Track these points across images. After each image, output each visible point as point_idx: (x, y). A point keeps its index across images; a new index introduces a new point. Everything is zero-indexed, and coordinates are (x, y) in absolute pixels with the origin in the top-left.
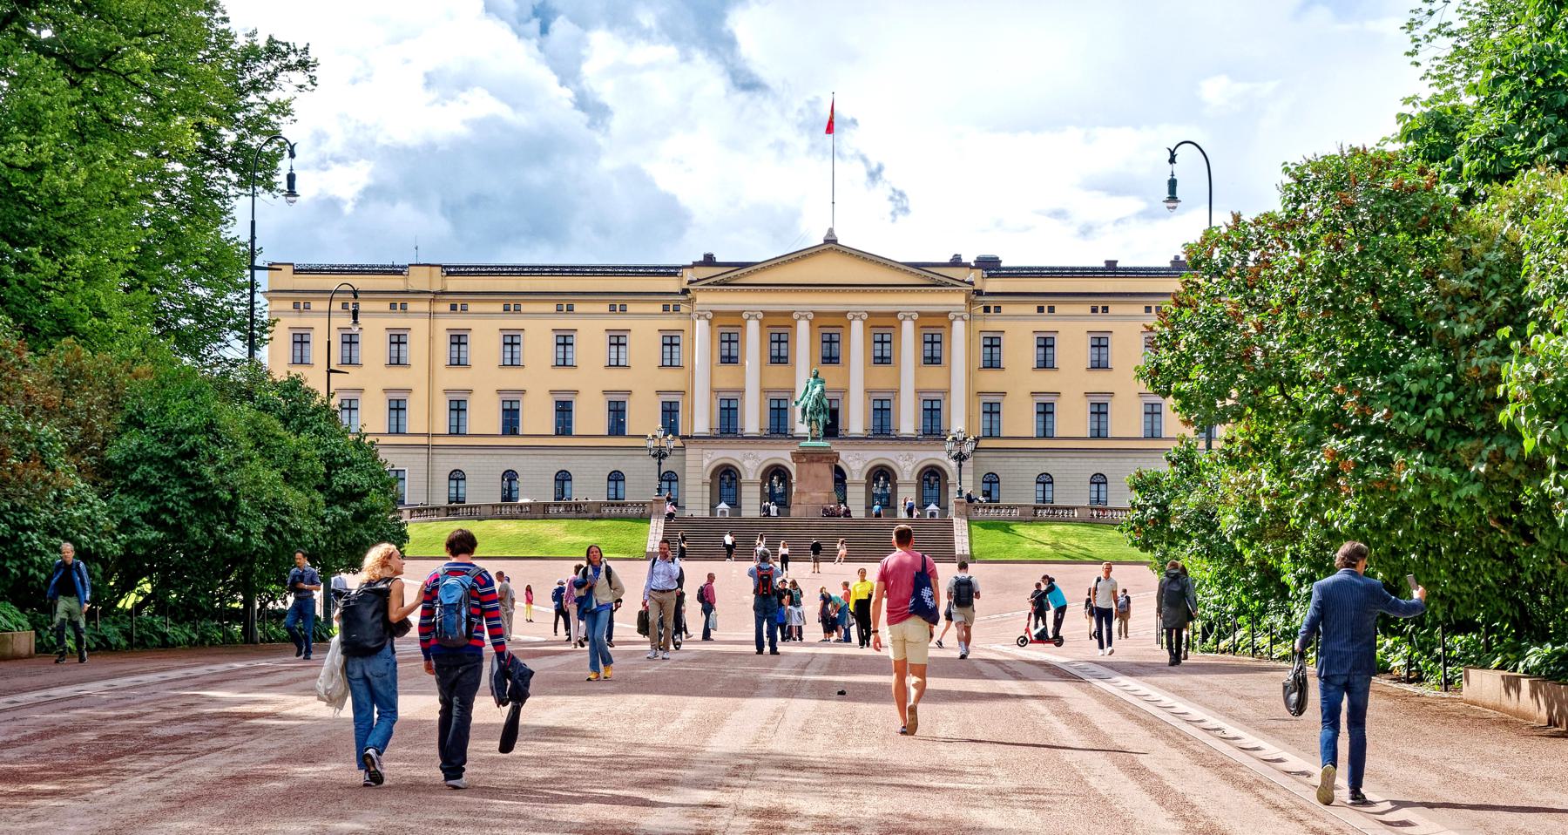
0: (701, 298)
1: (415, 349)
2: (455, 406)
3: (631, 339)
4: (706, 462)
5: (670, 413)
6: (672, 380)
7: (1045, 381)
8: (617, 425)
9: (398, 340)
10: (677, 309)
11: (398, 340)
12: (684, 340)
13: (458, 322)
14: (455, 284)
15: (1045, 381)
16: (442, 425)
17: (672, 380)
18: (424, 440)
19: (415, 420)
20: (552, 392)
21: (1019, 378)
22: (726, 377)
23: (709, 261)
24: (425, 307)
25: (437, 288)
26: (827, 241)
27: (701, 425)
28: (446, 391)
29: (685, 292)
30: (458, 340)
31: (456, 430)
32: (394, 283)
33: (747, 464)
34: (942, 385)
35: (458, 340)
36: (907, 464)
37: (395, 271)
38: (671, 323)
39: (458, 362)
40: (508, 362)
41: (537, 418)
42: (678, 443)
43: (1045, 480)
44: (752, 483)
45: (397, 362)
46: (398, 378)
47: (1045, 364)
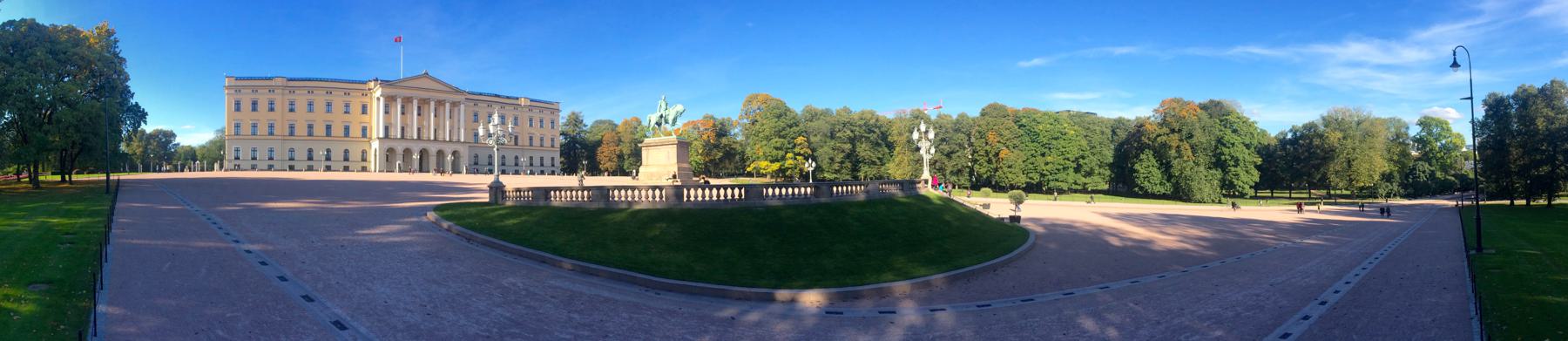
1: (277, 107)
13: (292, 97)
16: (287, 132)
39: (292, 110)
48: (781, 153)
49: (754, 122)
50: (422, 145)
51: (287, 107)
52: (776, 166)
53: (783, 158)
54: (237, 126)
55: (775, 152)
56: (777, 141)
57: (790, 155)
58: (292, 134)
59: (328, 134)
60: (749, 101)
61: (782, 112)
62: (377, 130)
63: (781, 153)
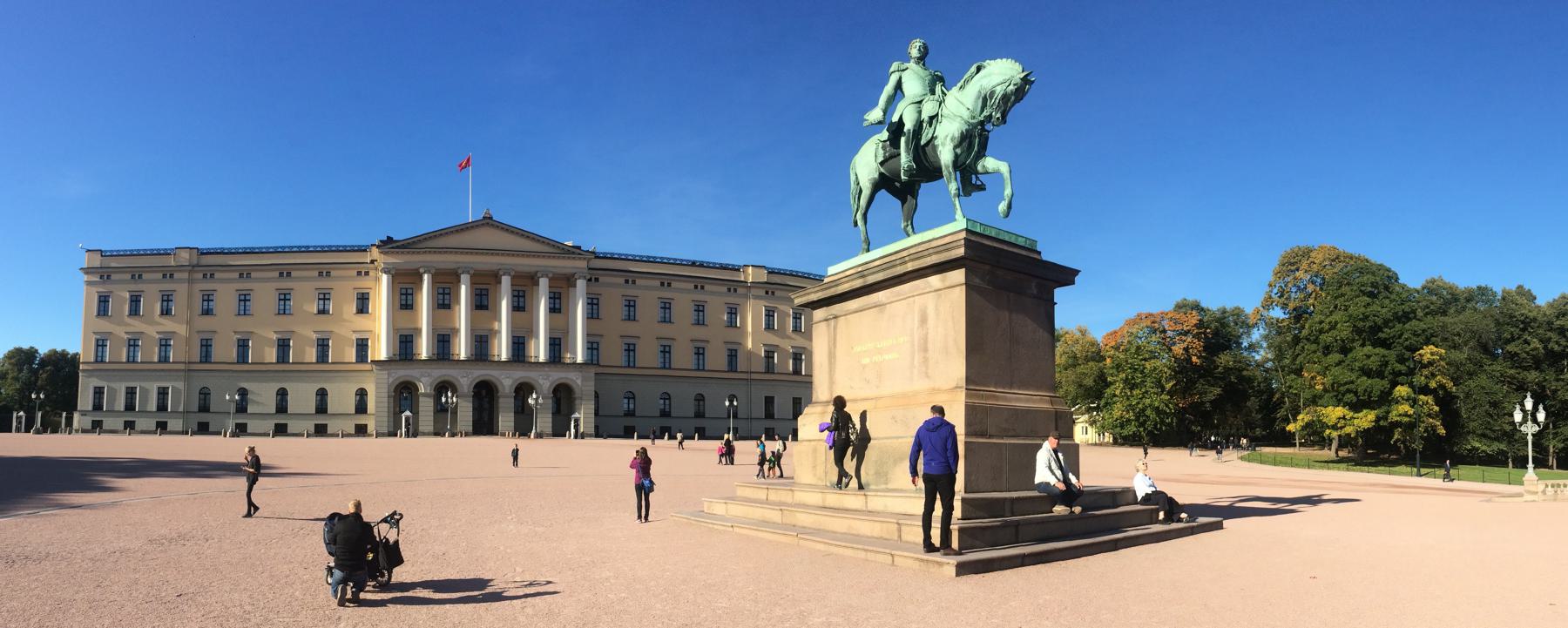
10: (367, 273)
16: (196, 355)
18: (182, 367)
23: (390, 239)
38: (364, 283)
39: (207, 312)
43: (631, 396)
44: (425, 395)
45: (166, 312)
48: (1379, 385)
49: (1299, 315)
50: (558, 376)
51: (198, 305)
52: (1366, 419)
53: (1386, 399)
54: (101, 344)
55: (1364, 382)
56: (1366, 353)
57: (1402, 390)
58: (206, 357)
59: (242, 357)
60: (1290, 264)
61: (1380, 283)
62: (381, 349)
63: (1379, 385)
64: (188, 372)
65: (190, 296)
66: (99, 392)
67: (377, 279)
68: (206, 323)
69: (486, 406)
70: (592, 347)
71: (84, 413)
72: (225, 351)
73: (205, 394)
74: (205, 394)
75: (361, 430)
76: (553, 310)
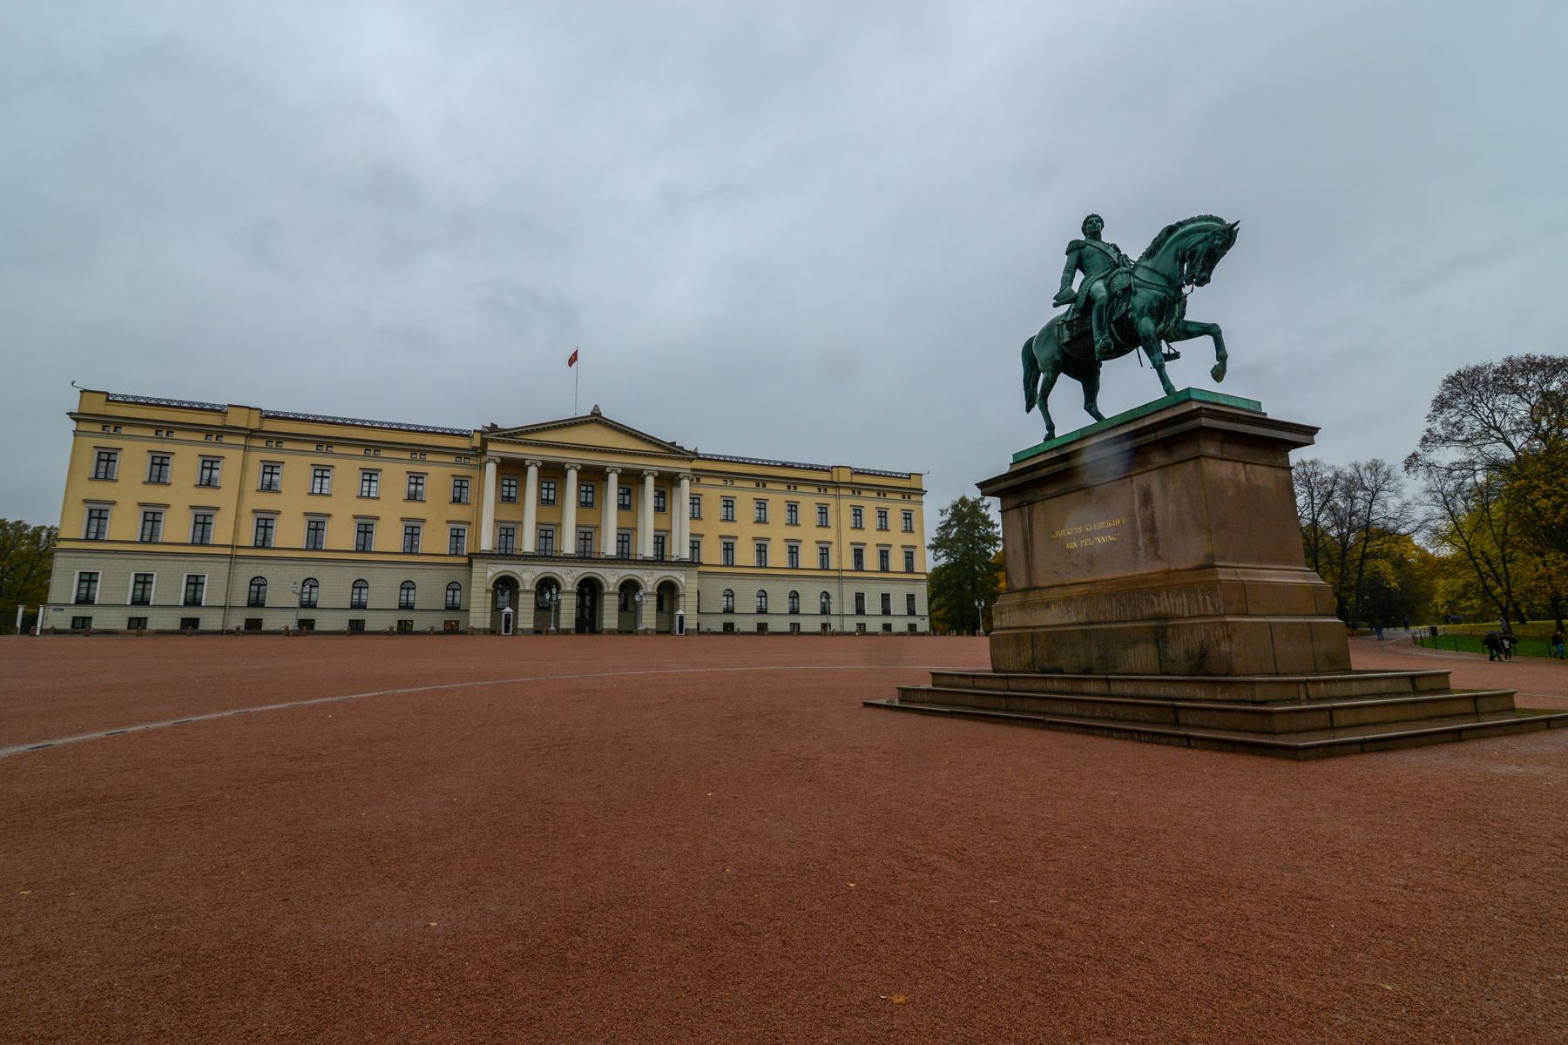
0: (491, 447)
1: (228, 473)
2: (262, 523)
3: (427, 480)
4: (490, 574)
5: (457, 536)
6: (458, 512)
7: (728, 529)
8: (411, 547)
9: (210, 463)
11: (210, 463)
12: (472, 484)
14: (270, 426)
15: (728, 529)
16: (248, 537)
17: (458, 512)
18: (228, 551)
19: (221, 532)
20: (355, 517)
21: (713, 530)
22: (508, 513)
24: (241, 441)
25: (254, 425)
26: (593, 414)
27: (486, 544)
28: (254, 511)
29: (474, 449)
30: (270, 468)
31: (263, 543)
32: (214, 420)
33: (525, 576)
34: (666, 527)
35: (270, 468)
36: (650, 580)
37: (213, 410)
39: (269, 488)
40: (317, 491)
41: (341, 536)
42: (465, 560)
43: (730, 594)
44: (528, 592)
45: (209, 483)
46: (206, 498)
47: (729, 519)
51: (255, 476)
54: (98, 514)
64: (234, 556)
65: (244, 467)
66: (89, 579)
67: (483, 467)
68: (267, 502)
69: (588, 603)
70: (695, 546)
71: (60, 607)
72: (289, 533)
73: (258, 583)
74: (258, 583)
75: (452, 629)
76: (658, 509)
